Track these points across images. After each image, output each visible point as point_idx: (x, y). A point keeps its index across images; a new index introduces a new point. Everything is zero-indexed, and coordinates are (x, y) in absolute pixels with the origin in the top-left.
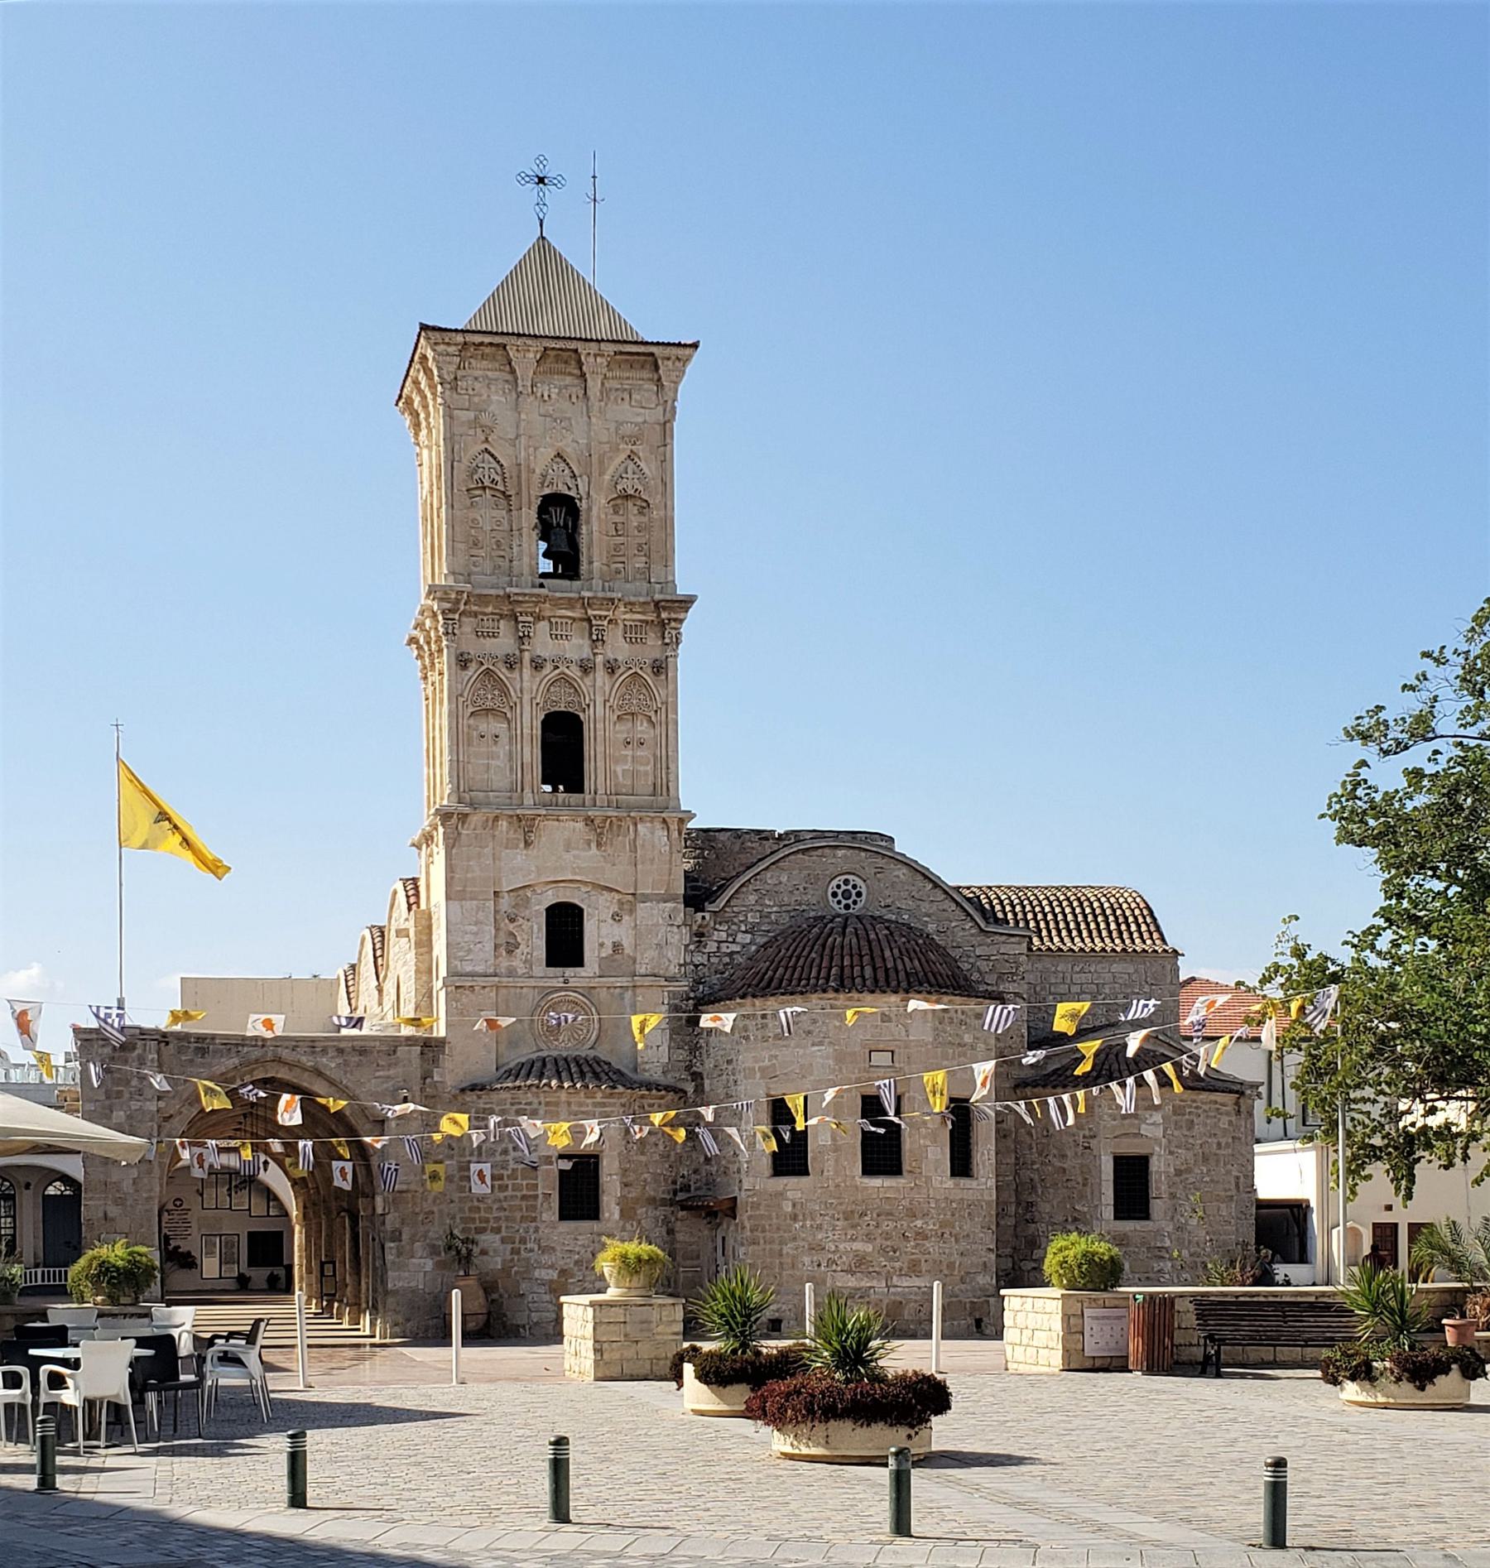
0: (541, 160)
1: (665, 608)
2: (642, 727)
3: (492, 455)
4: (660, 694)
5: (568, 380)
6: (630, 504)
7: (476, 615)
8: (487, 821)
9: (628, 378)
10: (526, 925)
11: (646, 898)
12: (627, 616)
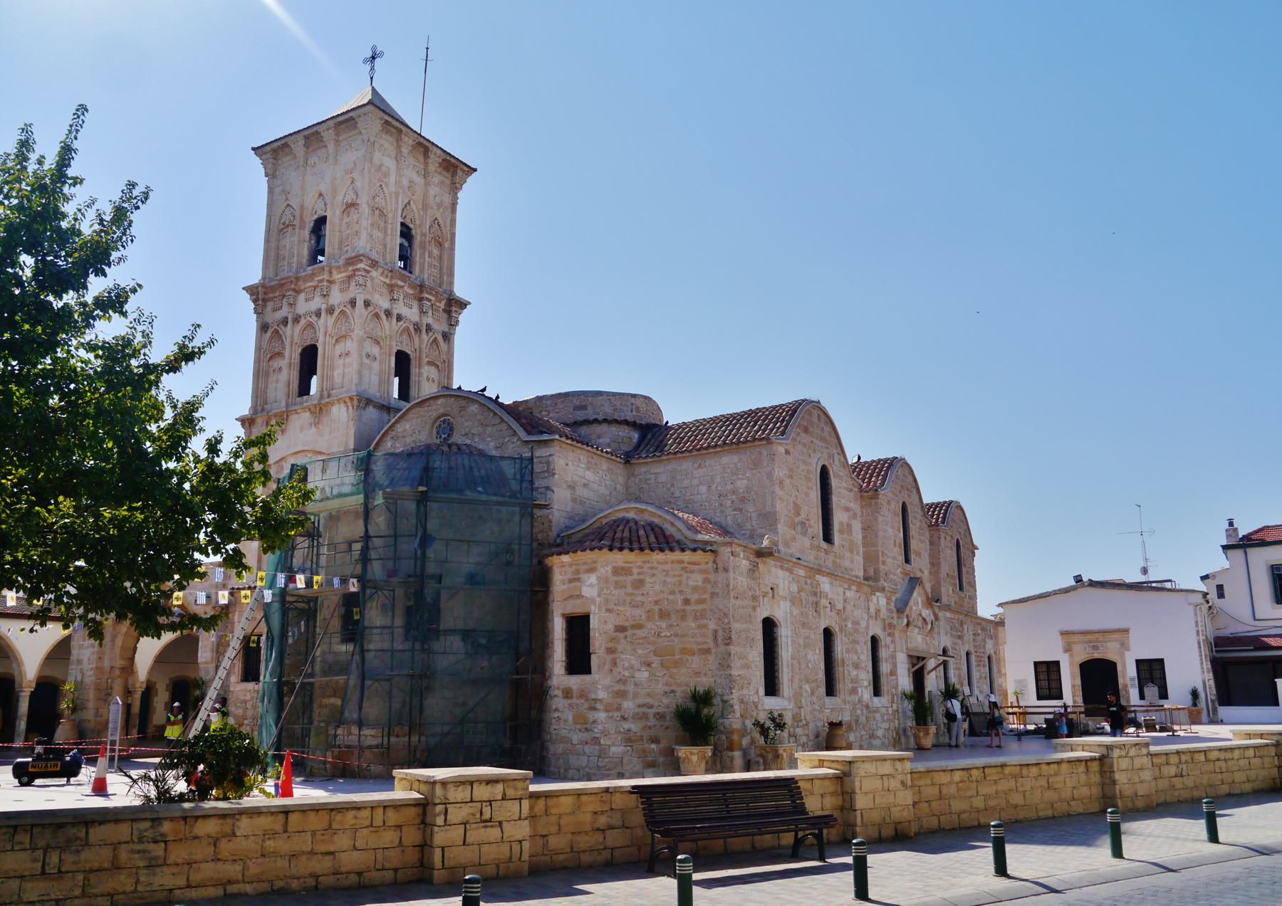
0: (374, 48)
6: (353, 209)
7: (272, 299)
12: (340, 276)
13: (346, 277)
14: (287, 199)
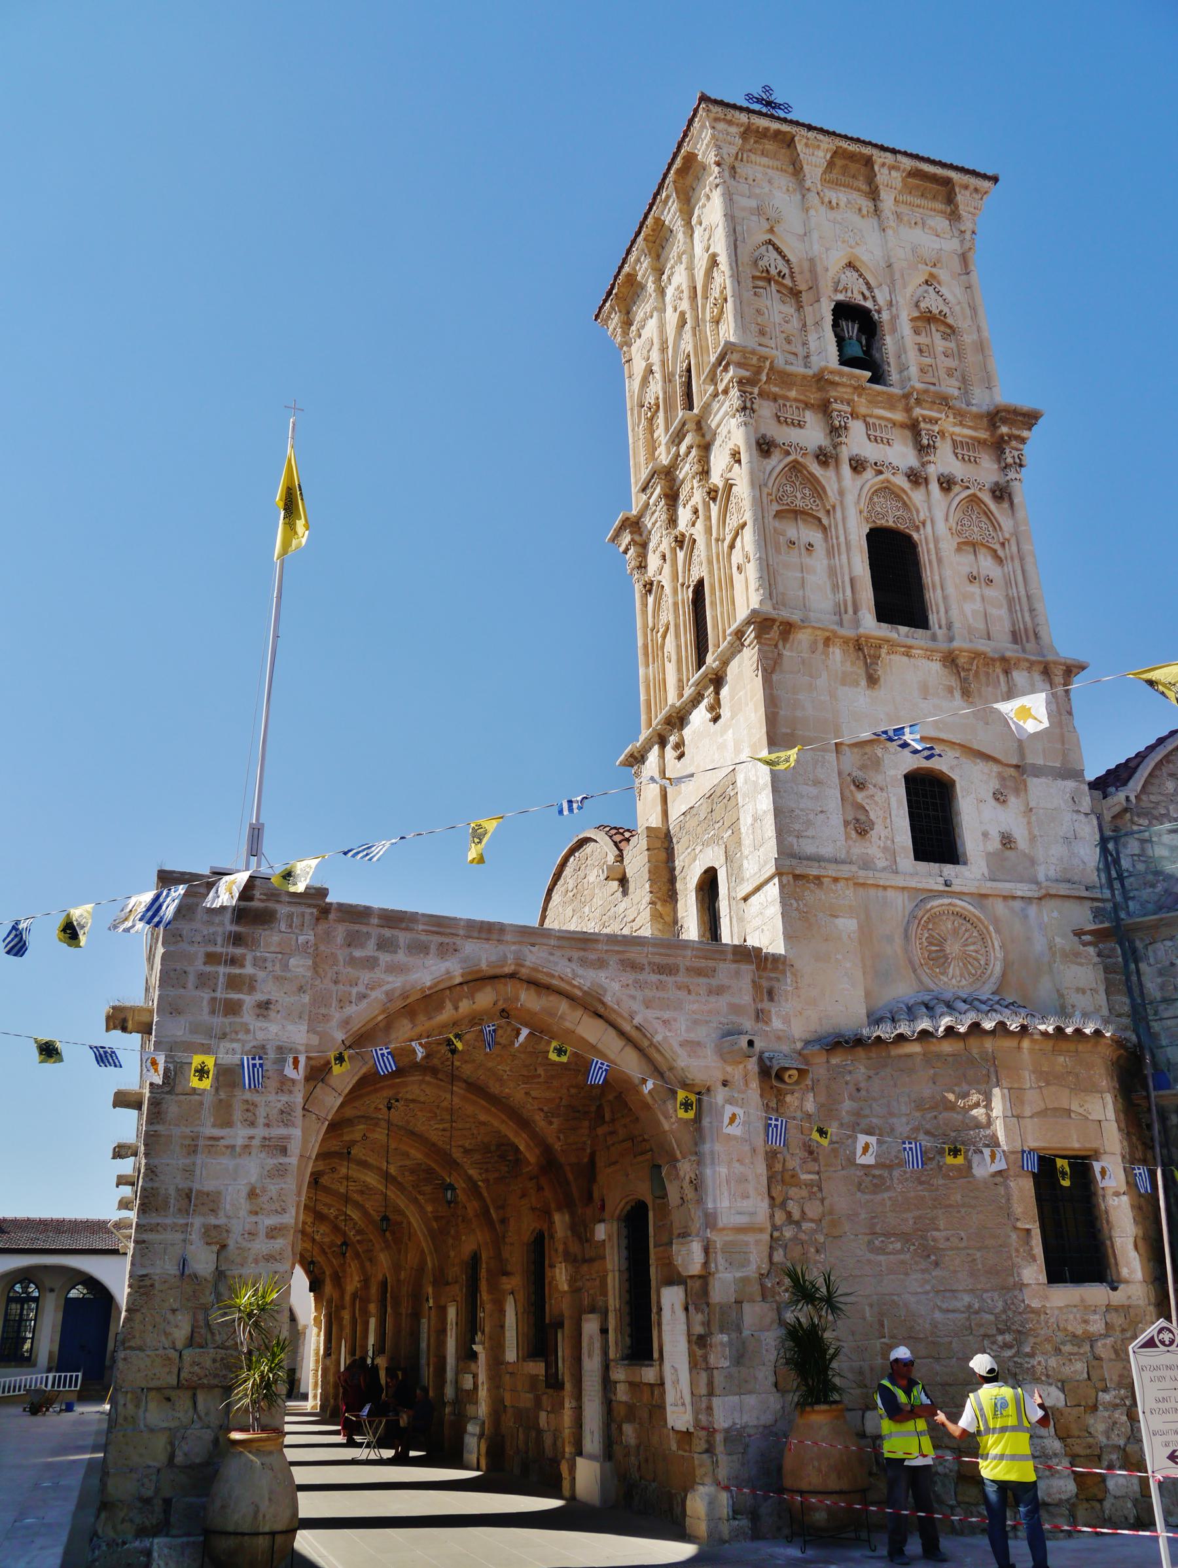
1: (1004, 421)
2: (986, 564)
3: (777, 249)
4: (1006, 523)
5: (855, 195)
8: (815, 642)
9: (918, 206)
10: (880, 797)
11: (1038, 772)
12: (957, 430)
13: (972, 438)
14: (771, 231)
